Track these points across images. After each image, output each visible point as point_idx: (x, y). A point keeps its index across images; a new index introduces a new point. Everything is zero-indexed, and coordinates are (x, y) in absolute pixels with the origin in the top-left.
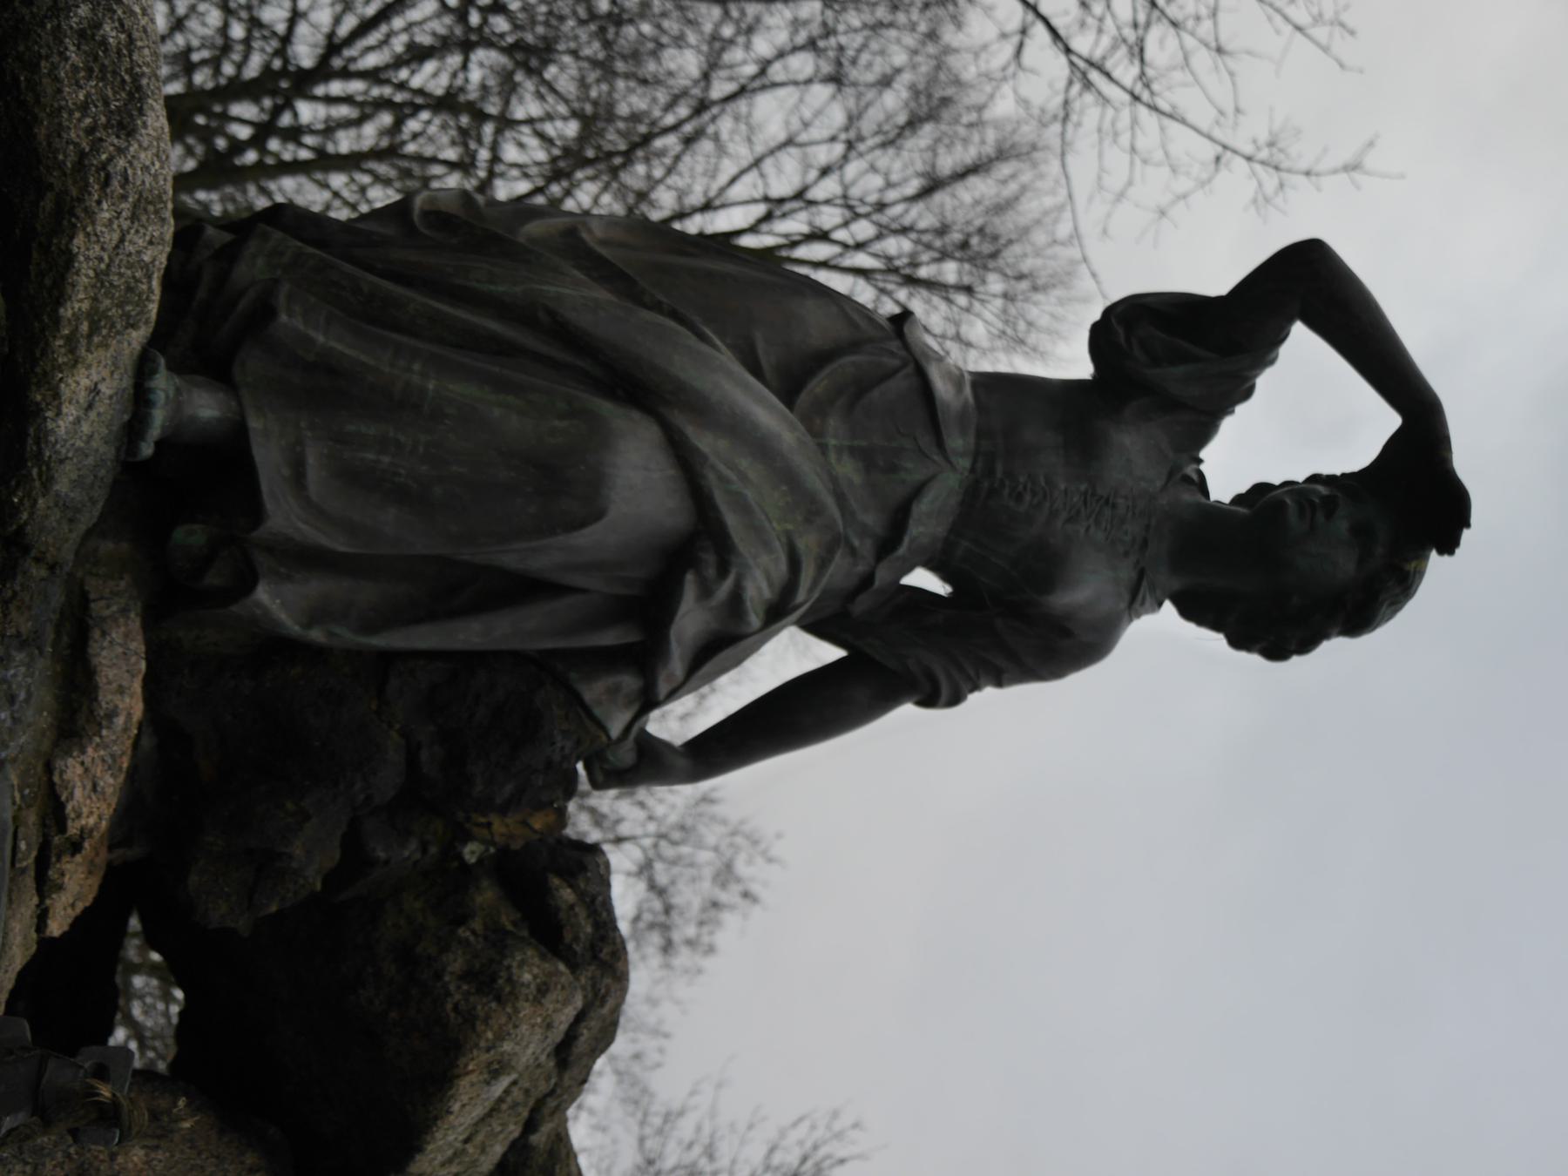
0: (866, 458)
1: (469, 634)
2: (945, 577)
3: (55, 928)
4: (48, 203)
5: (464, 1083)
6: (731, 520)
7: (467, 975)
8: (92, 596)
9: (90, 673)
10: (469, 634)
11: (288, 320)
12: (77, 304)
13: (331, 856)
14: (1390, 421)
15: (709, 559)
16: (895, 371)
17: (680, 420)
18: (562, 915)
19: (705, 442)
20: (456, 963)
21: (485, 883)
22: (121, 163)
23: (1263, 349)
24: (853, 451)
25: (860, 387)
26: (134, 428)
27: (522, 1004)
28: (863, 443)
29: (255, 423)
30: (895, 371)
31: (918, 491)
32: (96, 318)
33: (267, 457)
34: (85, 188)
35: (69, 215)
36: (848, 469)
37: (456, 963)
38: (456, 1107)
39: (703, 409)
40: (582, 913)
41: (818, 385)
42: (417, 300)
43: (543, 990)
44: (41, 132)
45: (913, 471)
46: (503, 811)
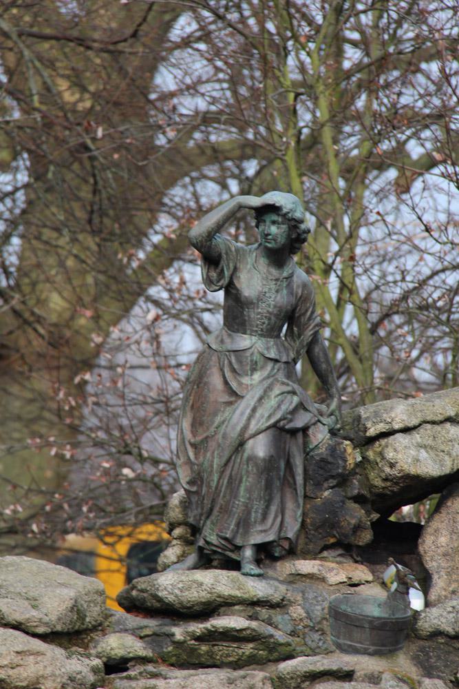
0: (254, 370)
1: (300, 479)
5: (419, 472)
6: (272, 421)
10: (300, 479)
12: (238, 593)
15: (282, 423)
19: (253, 427)
20: (387, 470)
25: (234, 371)
31: (263, 355)
33: (258, 539)
36: (257, 376)
41: (234, 385)
45: (256, 357)
46: (346, 461)
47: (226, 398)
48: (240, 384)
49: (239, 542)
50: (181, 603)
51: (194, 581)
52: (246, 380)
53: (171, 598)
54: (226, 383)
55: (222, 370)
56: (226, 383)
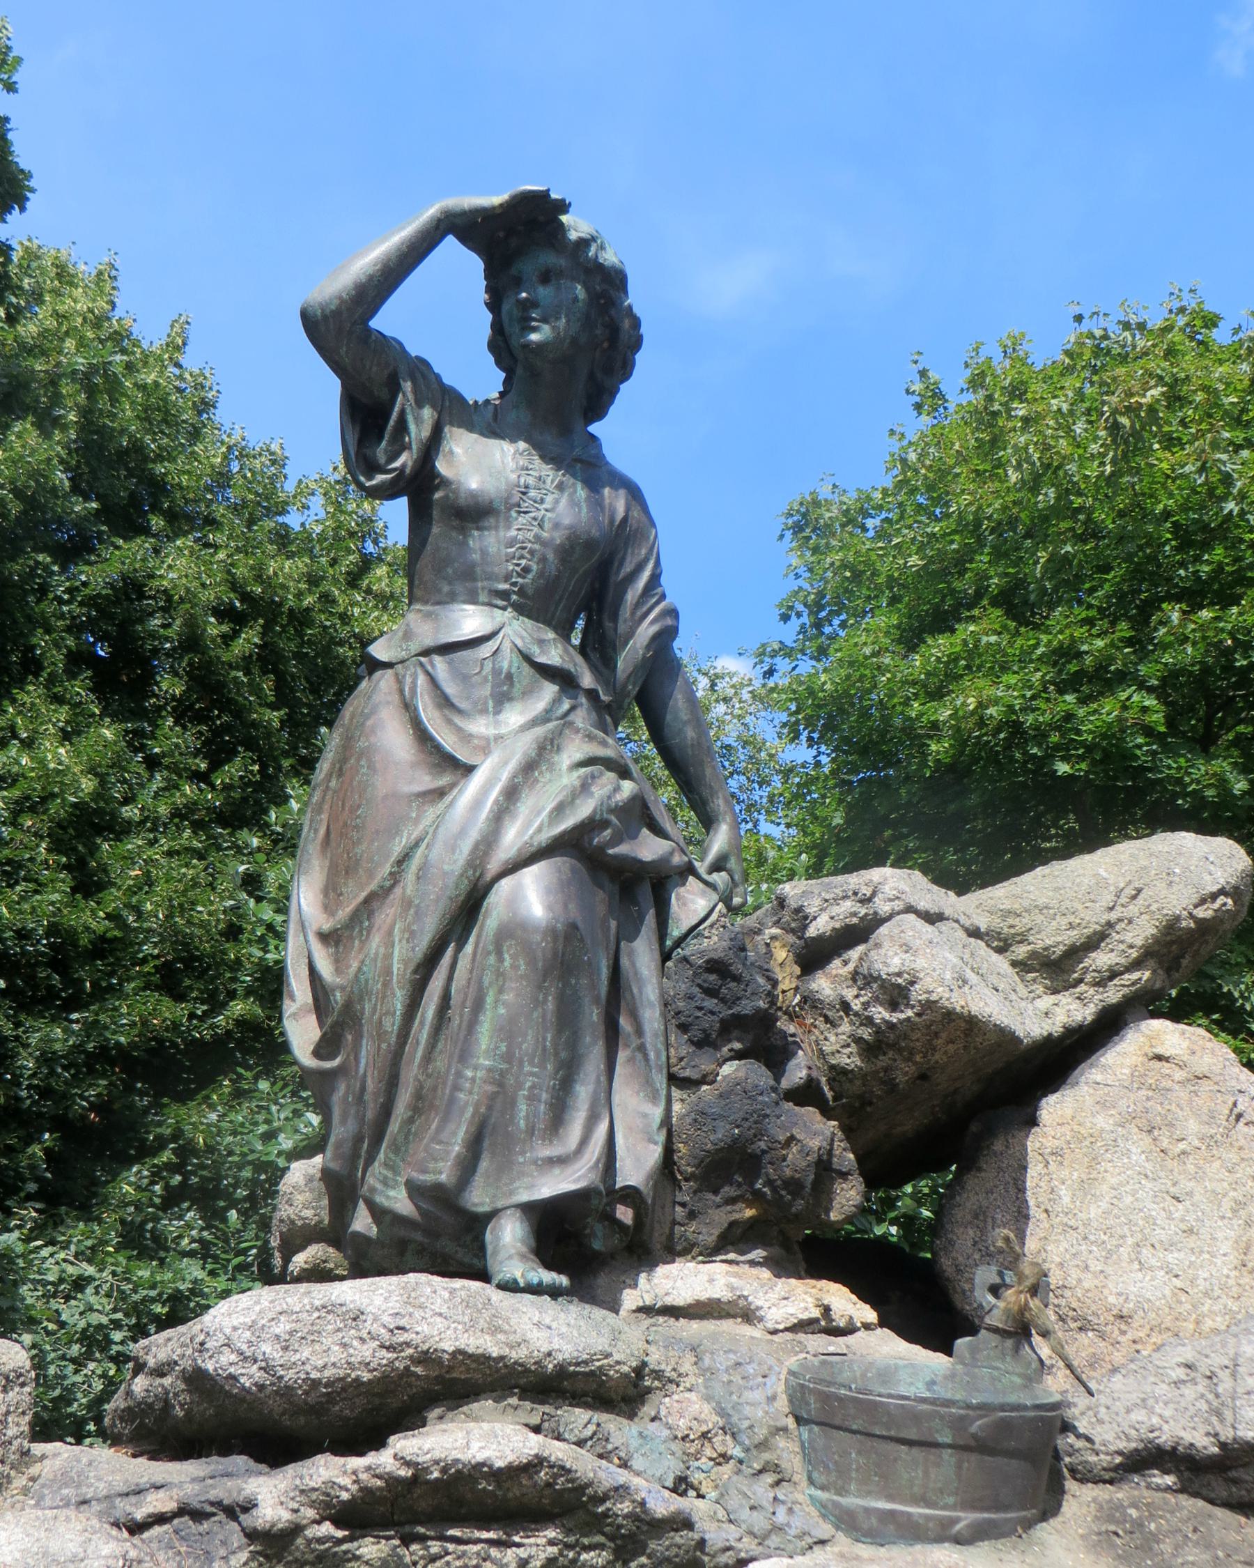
0: (502, 699)
2: (577, 617)
3: (871, 1316)
4: (419, 1370)
7: (893, 1006)
8: (641, 1304)
9: (698, 1304)
11: (444, 1173)
13: (811, 1113)
14: (451, 242)
16: (428, 673)
17: (493, 867)
18: (838, 925)
19: (513, 838)
21: (814, 986)
22: (386, 1319)
23: (387, 347)
24: (497, 712)
25: (445, 702)
26: (554, 1292)
27: (917, 966)
28: (491, 704)
29: (524, 1197)
30: (428, 673)
31: (527, 658)
32: (495, 1330)
33: (550, 1186)
34: (408, 1344)
35: (425, 1358)
36: (514, 717)
37: (880, 1013)
38: (988, 1010)
39: (489, 841)
40: (835, 910)
41: (447, 740)
42: (411, 1074)
43: (907, 948)
44: (366, 1376)
46: (775, 983)
47: (425, 781)
48: (466, 737)
49: (478, 1198)
50: (286, 1392)
51: (328, 1309)
52: (480, 726)
53: (250, 1376)
54: (423, 736)
55: (408, 707)
56: (423, 736)
